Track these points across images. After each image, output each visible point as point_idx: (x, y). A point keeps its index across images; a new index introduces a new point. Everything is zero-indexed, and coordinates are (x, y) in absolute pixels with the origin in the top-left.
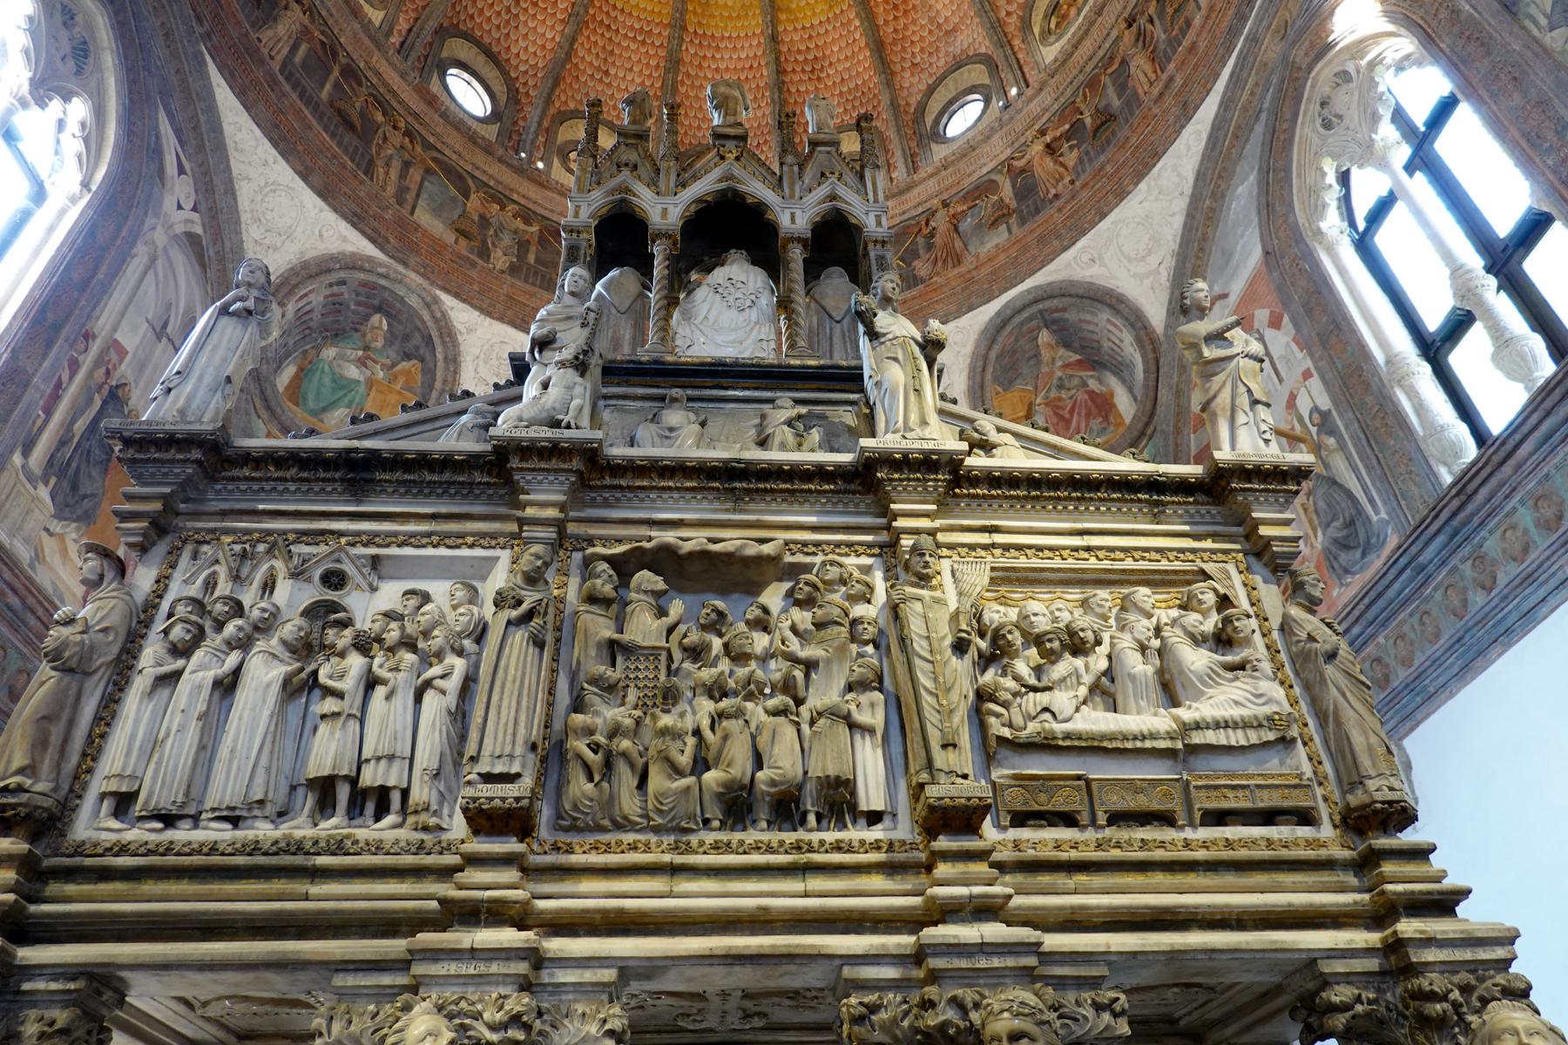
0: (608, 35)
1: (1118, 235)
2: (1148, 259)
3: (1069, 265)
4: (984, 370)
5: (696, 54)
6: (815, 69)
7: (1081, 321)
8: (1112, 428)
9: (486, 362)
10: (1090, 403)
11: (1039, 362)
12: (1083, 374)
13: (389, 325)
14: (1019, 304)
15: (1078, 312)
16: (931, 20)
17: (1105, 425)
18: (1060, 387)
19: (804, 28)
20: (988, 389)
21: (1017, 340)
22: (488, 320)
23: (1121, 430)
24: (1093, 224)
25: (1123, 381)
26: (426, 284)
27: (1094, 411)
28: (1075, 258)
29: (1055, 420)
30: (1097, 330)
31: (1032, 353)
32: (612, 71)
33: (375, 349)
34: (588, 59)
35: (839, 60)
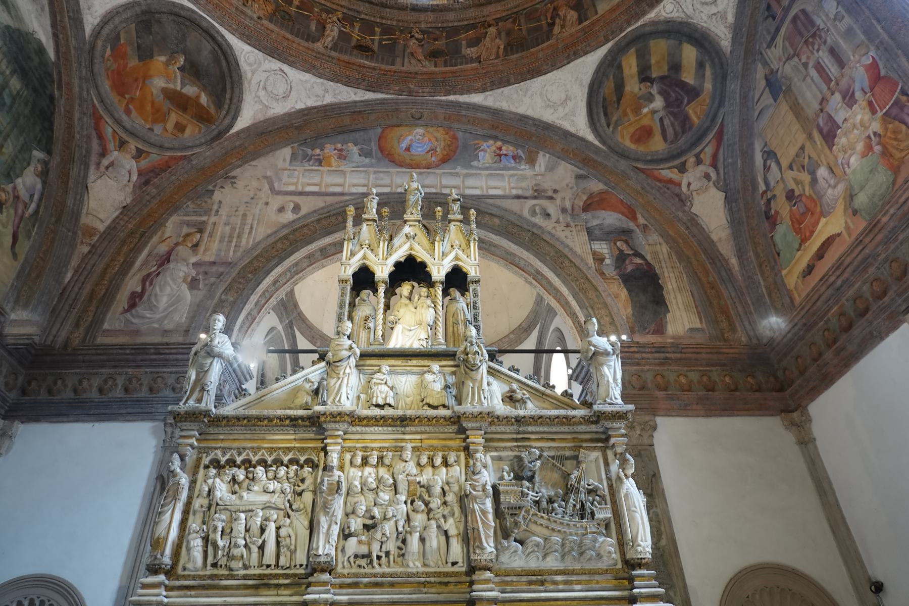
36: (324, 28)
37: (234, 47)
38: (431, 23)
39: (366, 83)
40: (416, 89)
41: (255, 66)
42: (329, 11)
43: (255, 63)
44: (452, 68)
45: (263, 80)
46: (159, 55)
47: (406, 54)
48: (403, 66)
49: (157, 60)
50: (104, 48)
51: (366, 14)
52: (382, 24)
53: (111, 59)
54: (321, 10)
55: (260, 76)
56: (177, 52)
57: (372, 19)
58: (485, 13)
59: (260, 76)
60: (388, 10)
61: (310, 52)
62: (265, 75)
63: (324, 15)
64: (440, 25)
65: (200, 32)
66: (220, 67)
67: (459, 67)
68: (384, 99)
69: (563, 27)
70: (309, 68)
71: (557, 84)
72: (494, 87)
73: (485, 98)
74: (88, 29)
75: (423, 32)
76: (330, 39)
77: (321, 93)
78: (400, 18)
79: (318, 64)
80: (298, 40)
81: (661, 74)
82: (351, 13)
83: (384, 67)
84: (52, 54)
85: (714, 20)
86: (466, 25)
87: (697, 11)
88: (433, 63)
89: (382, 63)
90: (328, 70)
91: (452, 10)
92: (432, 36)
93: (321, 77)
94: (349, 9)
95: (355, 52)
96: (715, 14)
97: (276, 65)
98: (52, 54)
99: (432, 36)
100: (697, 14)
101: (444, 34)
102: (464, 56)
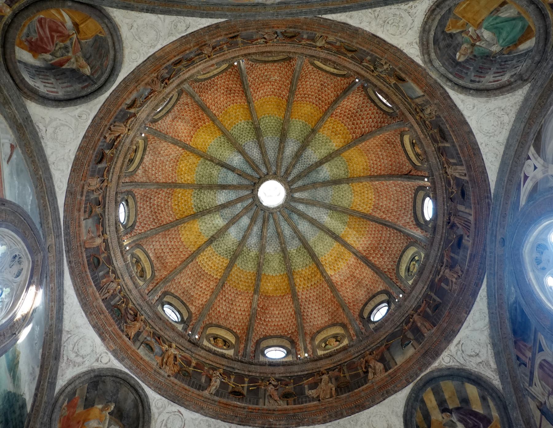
0: (320, 97)
1: (73, 132)
2: (53, 129)
3: (91, 110)
4: (114, 43)
5: (282, 91)
6: (229, 91)
7: (71, 86)
8: (24, 39)
9: (406, 25)
10: (45, 46)
11: (84, 56)
12: (57, 60)
13: (456, 55)
14: (108, 85)
15: (75, 90)
16: (184, 119)
17: (29, 38)
18: (66, 48)
19: (237, 103)
20: (107, 33)
21: (102, 64)
22: (399, 47)
23: (17, 41)
24: (88, 131)
25: (32, 66)
26: (428, 70)
27: (39, 43)
28: (89, 115)
29: (60, 29)
30: (61, 85)
31: (90, 60)
32: (319, 85)
33: (468, 43)
34: (329, 91)
35: (220, 96)
36: (211, 380)
37: (150, 396)
38: (282, 373)
39: (238, 419)
41: (161, 409)
42: (214, 369)
43: (162, 407)
45: (165, 419)
46: (98, 404)
47: (266, 396)
48: (264, 405)
49: (96, 408)
50: (64, 400)
52: (249, 376)
53: (66, 408)
54: (209, 368)
55: (164, 416)
56: (110, 402)
57: (243, 372)
58: (319, 366)
59: (164, 416)
60: (253, 366)
61: (200, 398)
62: (167, 415)
63: (211, 372)
64: (288, 375)
65: (129, 387)
66: (138, 411)
67: (305, 404)
69: (374, 374)
70: (198, 409)
72: (332, 419)
74: (57, 389)
75: (277, 380)
76: (214, 388)
78: (261, 371)
79: (205, 406)
81: (456, 406)
82: (228, 369)
83: (251, 406)
84: (29, 408)
85: (481, 366)
86: (307, 374)
87: (467, 361)
88: (285, 402)
89: (250, 404)
90: (211, 410)
91: (296, 365)
92: (284, 383)
93: (206, 416)
94: (228, 367)
95: (231, 396)
96: (480, 363)
97: (176, 407)
98: (29, 408)
99: (284, 383)
100: (468, 363)
101: (292, 381)
102: (308, 396)
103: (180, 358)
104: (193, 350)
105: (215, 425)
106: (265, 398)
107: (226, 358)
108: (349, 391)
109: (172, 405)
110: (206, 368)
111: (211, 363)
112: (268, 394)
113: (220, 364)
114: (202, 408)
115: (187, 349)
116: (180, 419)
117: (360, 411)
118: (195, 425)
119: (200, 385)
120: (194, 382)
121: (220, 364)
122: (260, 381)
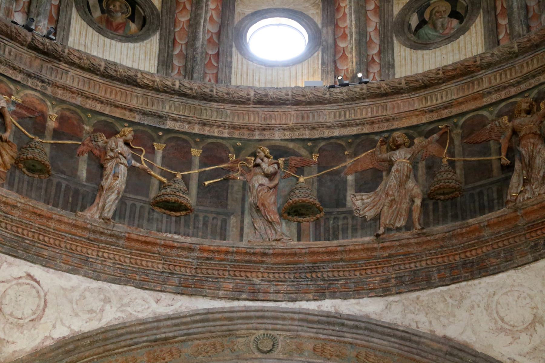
36: (102, 167)
38: (291, 129)
39: (175, 280)
40: (264, 286)
42: (112, 133)
44: (327, 243)
47: (247, 206)
51: (175, 120)
52: (203, 137)
57: (186, 128)
60: (214, 105)
61: (79, 232)
63: (102, 139)
64: (307, 134)
67: (341, 241)
68: (209, 312)
69: (526, 182)
71: (516, 294)
72: (402, 289)
73: (387, 307)
76: (113, 196)
77: (97, 305)
78: (236, 121)
79: (92, 254)
80: (58, 213)
82: (148, 121)
83: (207, 243)
86: (357, 136)
88: (294, 225)
89: (204, 236)
90: (109, 263)
91: (330, 102)
92: (294, 161)
93: (97, 279)
94: (144, 113)
95: (158, 213)
101: (315, 157)
102: (351, 212)
103: (14, 113)
104: (46, 75)
105: (121, 298)
106: (243, 213)
107: (138, 85)
108: (455, 218)
109: (10, 264)
110: (87, 128)
111: (98, 107)
112: (250, 200)
113: (125, 108)
114: (86, 261)
115: (29, 75)
116: (34, 292)
117: (473, 277)
118: (71, 302)
119: (76, 193)
120: (59, 185)
121: (125, 108)
122: (232, 157)
